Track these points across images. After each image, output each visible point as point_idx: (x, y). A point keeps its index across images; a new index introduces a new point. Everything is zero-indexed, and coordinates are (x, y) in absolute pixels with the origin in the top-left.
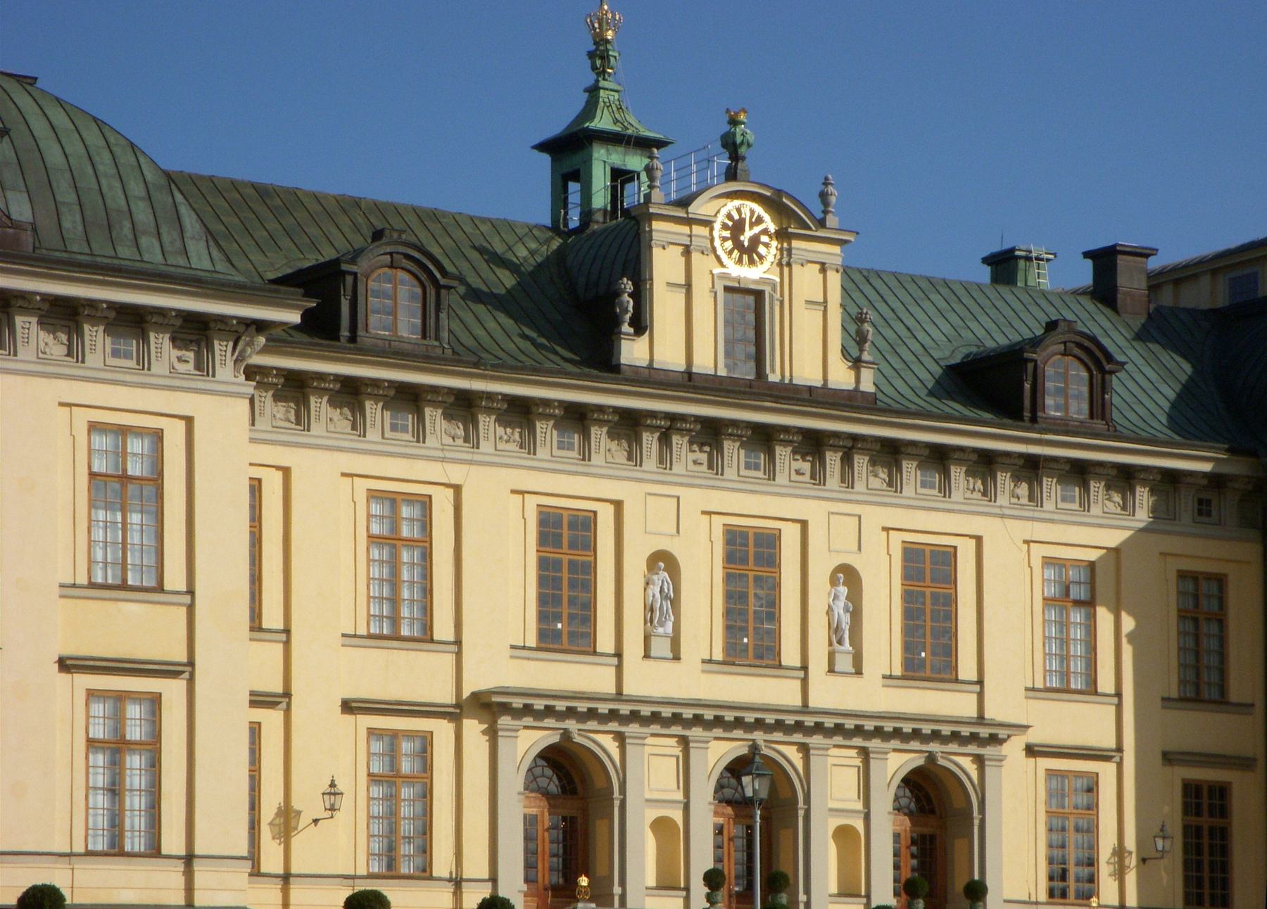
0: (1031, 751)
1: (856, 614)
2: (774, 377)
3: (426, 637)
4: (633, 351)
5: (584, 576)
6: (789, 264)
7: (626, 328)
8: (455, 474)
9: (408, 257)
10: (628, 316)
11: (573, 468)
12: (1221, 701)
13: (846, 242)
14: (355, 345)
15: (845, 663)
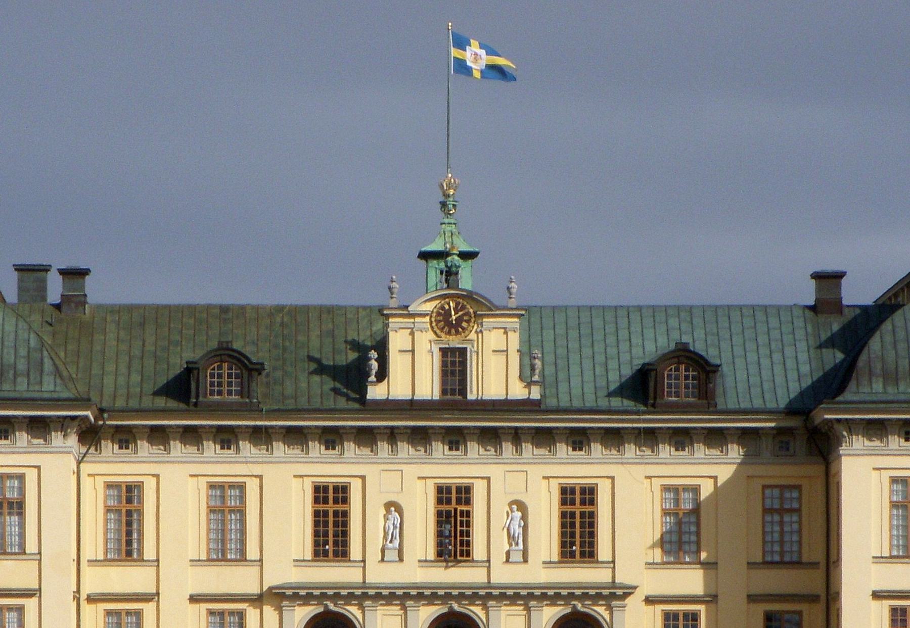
0: (650, 600)
1: (525, 529)
2: (471, 396)
3: (242, 558)
4: (376, 392)
5: (342, 521)
6: (481, 332)
7: (373, 378)
8: (257, 469)
9: (230, 356)
10: (374, 372)
11: (336, 460)
12: (798, 564)
13: (523, 315)
14: (197, 409)
15: (517, 556)
